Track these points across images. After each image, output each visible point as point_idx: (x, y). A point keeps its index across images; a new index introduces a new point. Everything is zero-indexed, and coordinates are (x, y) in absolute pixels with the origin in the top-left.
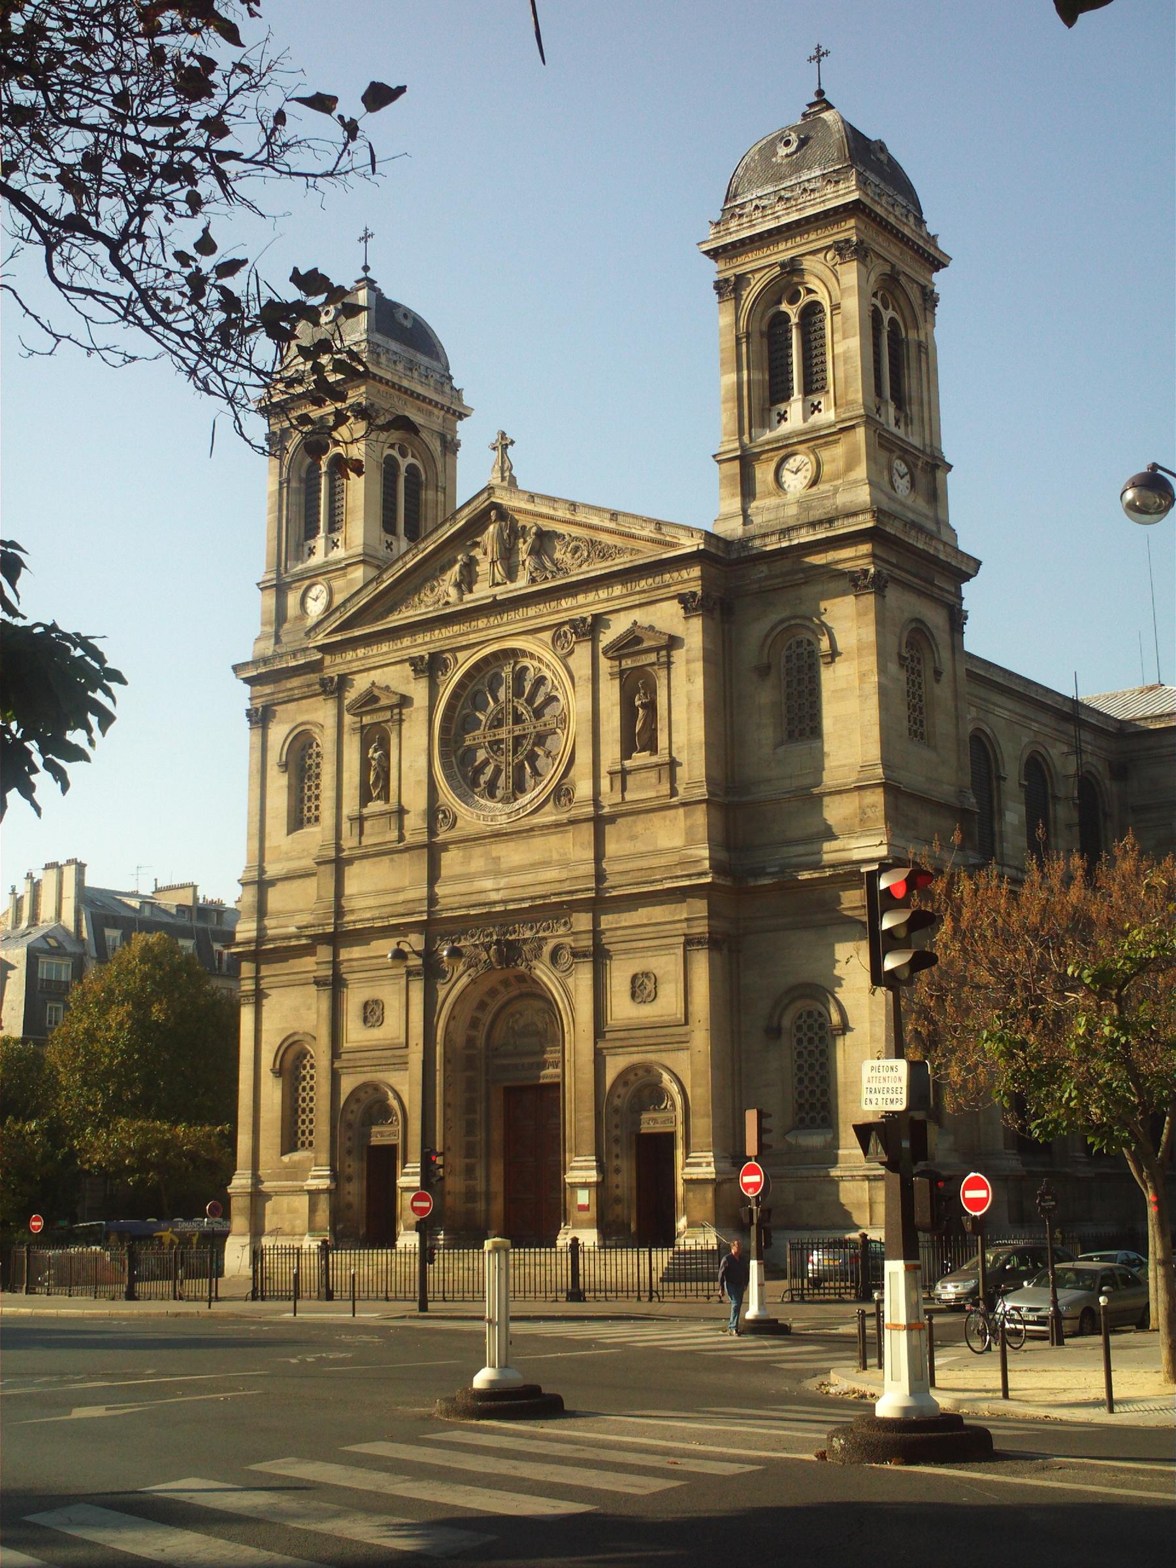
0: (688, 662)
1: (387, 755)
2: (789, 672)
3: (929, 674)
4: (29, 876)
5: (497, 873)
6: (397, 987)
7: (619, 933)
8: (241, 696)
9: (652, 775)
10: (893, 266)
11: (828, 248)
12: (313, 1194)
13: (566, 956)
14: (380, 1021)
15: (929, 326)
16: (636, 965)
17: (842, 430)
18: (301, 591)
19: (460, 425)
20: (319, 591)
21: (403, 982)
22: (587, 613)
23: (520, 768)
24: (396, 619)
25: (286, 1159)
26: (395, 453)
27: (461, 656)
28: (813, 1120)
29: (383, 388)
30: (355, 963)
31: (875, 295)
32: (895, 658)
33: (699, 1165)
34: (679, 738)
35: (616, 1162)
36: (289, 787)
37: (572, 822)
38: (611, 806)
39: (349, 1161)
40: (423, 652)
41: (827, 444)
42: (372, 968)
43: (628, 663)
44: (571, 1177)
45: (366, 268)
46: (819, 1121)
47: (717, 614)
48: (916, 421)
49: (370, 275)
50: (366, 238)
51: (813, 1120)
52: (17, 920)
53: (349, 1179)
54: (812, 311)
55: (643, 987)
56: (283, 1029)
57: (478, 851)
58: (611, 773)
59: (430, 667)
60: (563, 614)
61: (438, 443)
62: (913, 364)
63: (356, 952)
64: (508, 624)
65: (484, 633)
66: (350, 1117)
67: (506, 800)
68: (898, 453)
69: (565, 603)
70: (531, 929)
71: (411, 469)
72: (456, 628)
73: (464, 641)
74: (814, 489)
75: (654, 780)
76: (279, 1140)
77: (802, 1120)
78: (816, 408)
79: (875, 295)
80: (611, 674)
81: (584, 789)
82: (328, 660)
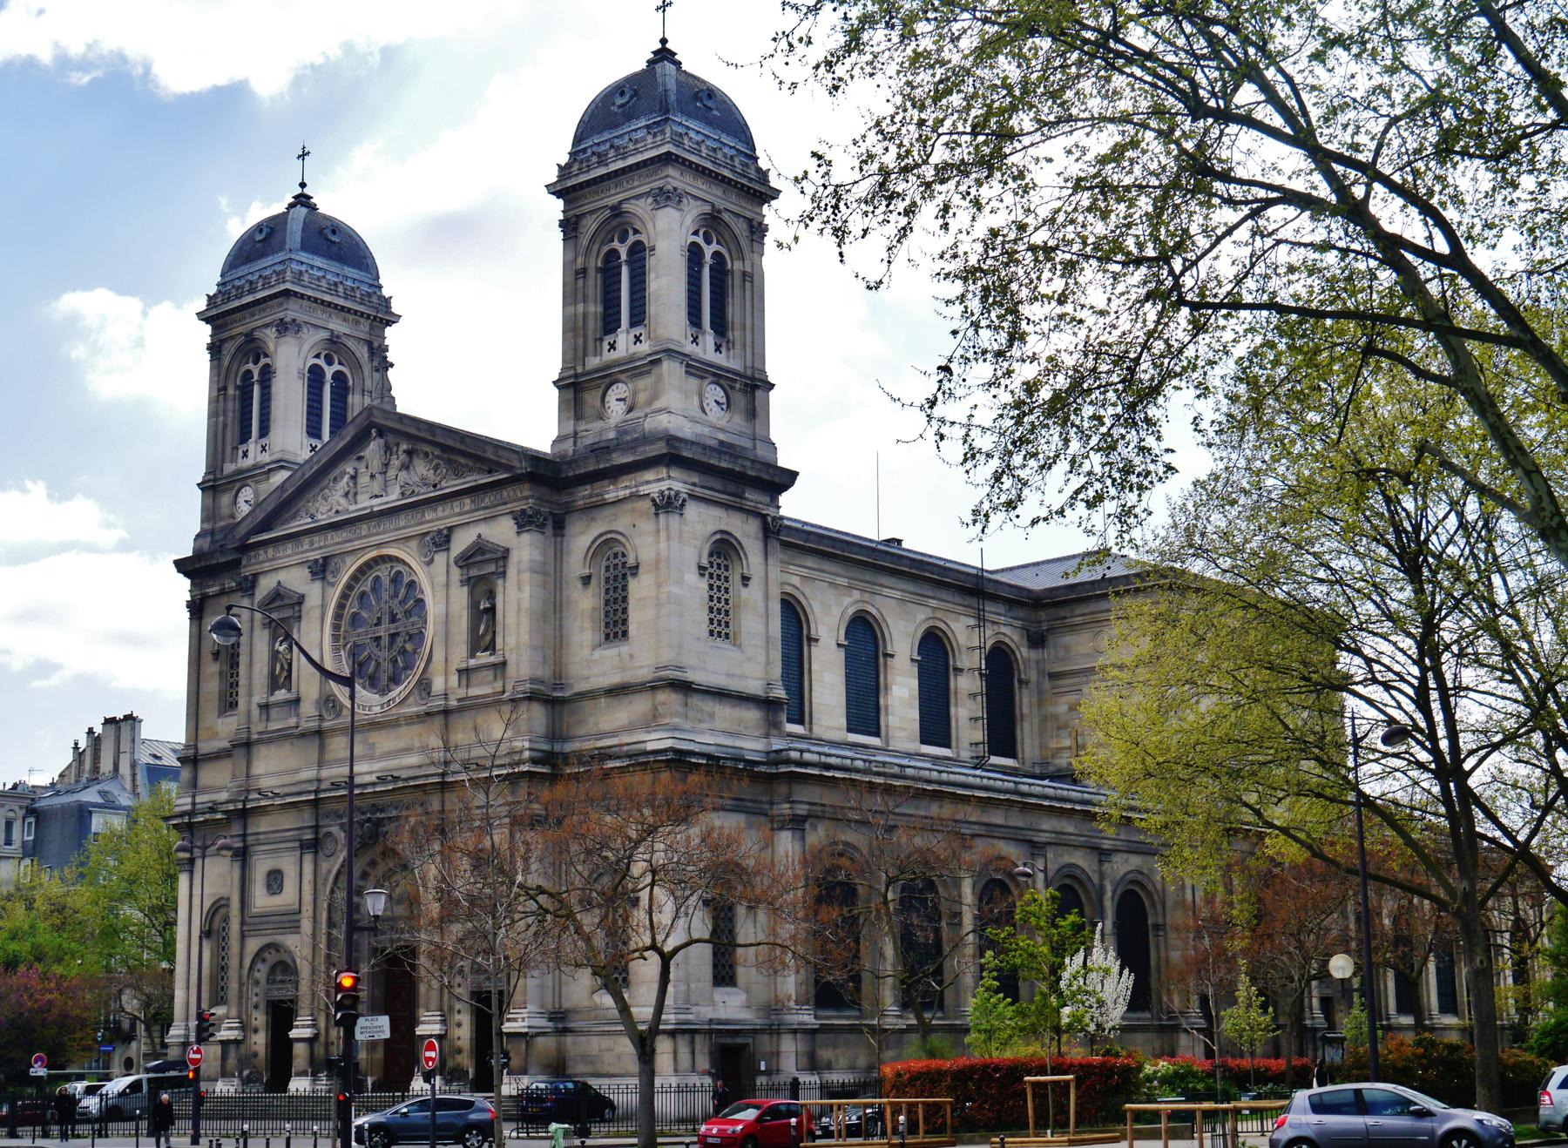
0: (519, 572)
2: (607, 579)
3: (735, 579)
4: (91, 731)
8: (182, 587)
9: (489, 674)
10: (713, 206)
11: (647, 194)
12: (225, 1044)
14: (281, 888)
15: (756, 256)
17: (652, 362)
19: (389, 331)
20: (247, 493)
21: (298, 853)
22: (442, 524)
24: (301, 523)
26: (321, 362)
27: (349, 560)
29: (305, 303)
31: (696, 233)
32: (695, 569)
33: (515, 1020)
34: (511, 640)
35: (457, 1017)
36: (221, 673)
38: (459, 700)
39: (255, 1014)
40: (315, 555)
41: (641, 374)
42: (276, 841)
43: (474, 572)
44: (421, 1030)
45: (303, 185)
47: (549, 530)
48: (738, 346)
49: (306, 191)
50: (303, 155)
52: (79, 775)
53: (256, 1031)
54: (639, 252)
59: (321, 570)
61: (365, 349)
62: (737, 292)
63: (261, 825)
64: (384, 533)
66: (257, 975)
67: (383, 692)
68: (711, 379)
69: (429, 516)
71: (338, 376)
73: (349, 547)
74: (631, 415)
78: (638, 339)
79: (696, 233)
81: (438, 685)
82: (244, 562)
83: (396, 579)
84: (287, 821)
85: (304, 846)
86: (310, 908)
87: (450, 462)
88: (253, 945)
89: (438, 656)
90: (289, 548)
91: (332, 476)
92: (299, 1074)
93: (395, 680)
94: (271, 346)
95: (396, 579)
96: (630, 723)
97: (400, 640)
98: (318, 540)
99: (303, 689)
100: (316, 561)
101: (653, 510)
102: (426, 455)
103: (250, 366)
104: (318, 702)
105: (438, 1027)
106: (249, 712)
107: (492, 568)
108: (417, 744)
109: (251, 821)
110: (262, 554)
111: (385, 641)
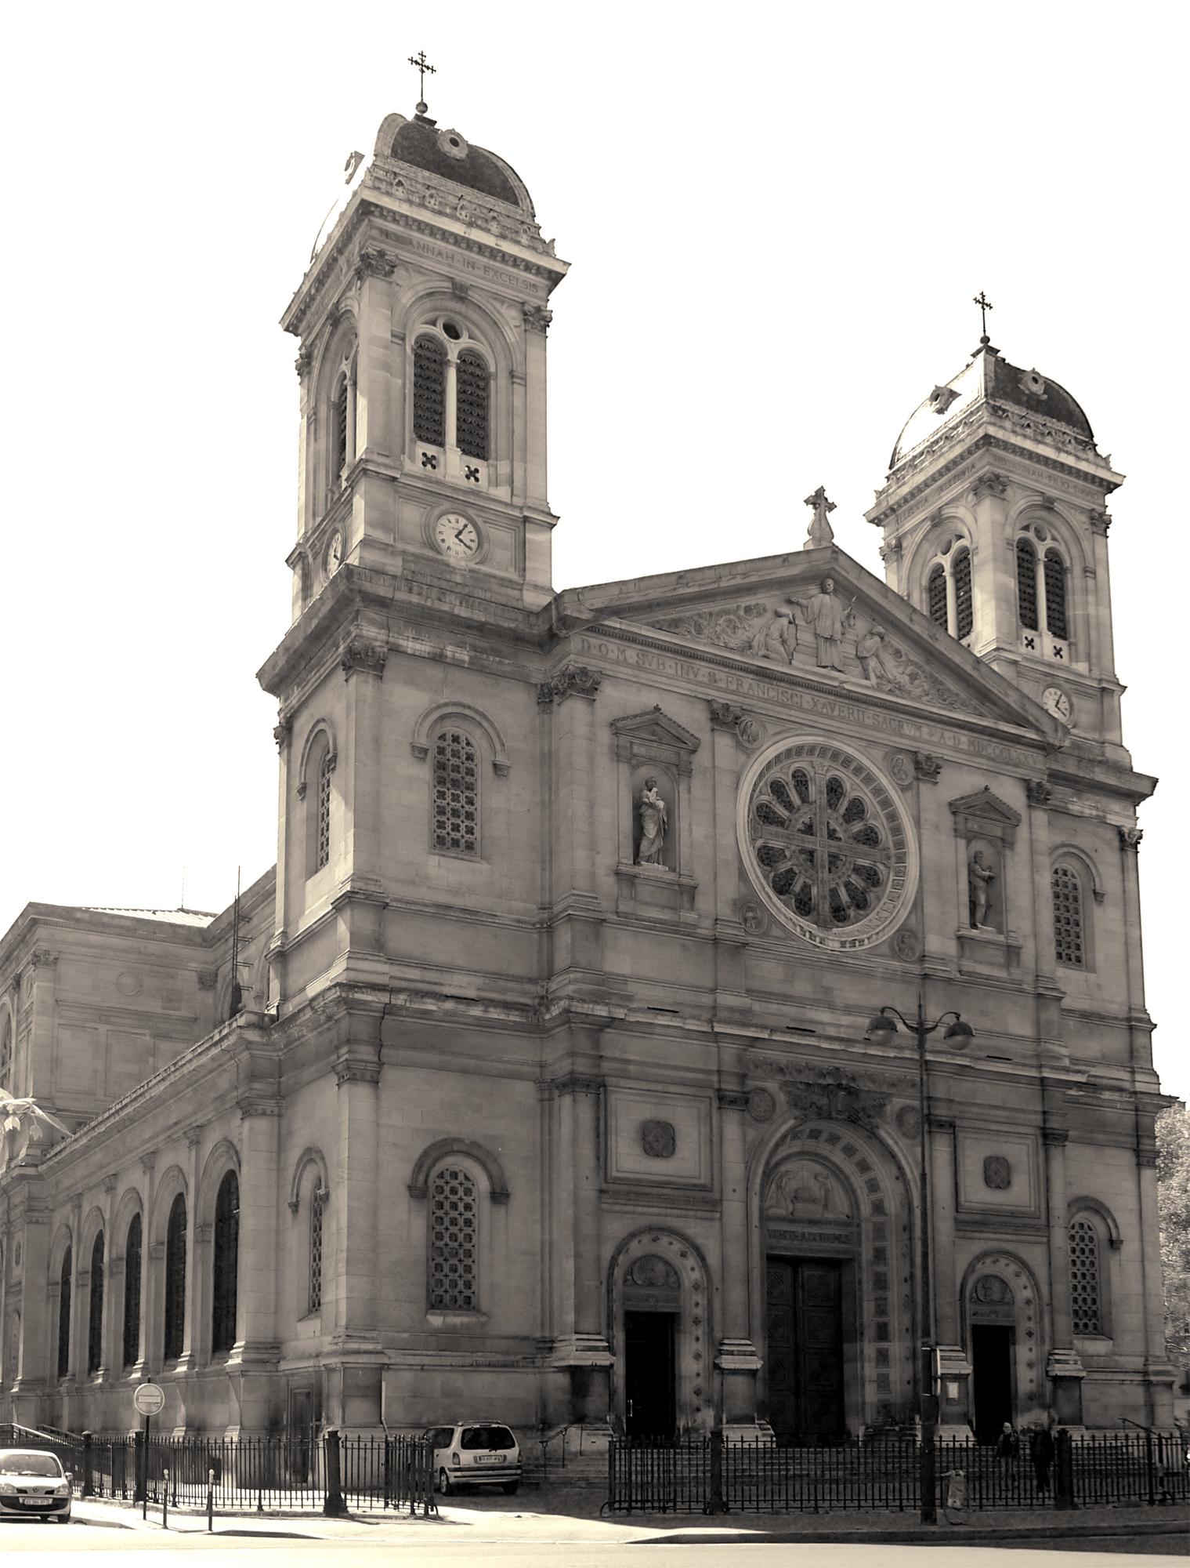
0: (1032, 852)
1: (670, 811)
5: (831, 1007)
7: (975, 1110)
16: (990, 1148)
21: (704, 1107)
28: (1086, 1326)
30: (632, 1068)
43: (973, 825)
46: (1091, 1328)
51: (1086, 1326)
55: (997, 1173)
58: (959, 938)
60: (906, 741)
65: (811, 717)
70: (874, 1082)
72: (772, 693)
75: (1002, 960)
77: (1076, 1325)
80: (955, 830)
85: (724, 1100)
88: (616, 1228)
89: (931, 907)
90: (671, 665)
92: (736, 1420)
93: (839, 915)
96: (1103, 1056)
99: (702, 876)
100: (727, 707)
104: (735, 903)
106: (592, 876)
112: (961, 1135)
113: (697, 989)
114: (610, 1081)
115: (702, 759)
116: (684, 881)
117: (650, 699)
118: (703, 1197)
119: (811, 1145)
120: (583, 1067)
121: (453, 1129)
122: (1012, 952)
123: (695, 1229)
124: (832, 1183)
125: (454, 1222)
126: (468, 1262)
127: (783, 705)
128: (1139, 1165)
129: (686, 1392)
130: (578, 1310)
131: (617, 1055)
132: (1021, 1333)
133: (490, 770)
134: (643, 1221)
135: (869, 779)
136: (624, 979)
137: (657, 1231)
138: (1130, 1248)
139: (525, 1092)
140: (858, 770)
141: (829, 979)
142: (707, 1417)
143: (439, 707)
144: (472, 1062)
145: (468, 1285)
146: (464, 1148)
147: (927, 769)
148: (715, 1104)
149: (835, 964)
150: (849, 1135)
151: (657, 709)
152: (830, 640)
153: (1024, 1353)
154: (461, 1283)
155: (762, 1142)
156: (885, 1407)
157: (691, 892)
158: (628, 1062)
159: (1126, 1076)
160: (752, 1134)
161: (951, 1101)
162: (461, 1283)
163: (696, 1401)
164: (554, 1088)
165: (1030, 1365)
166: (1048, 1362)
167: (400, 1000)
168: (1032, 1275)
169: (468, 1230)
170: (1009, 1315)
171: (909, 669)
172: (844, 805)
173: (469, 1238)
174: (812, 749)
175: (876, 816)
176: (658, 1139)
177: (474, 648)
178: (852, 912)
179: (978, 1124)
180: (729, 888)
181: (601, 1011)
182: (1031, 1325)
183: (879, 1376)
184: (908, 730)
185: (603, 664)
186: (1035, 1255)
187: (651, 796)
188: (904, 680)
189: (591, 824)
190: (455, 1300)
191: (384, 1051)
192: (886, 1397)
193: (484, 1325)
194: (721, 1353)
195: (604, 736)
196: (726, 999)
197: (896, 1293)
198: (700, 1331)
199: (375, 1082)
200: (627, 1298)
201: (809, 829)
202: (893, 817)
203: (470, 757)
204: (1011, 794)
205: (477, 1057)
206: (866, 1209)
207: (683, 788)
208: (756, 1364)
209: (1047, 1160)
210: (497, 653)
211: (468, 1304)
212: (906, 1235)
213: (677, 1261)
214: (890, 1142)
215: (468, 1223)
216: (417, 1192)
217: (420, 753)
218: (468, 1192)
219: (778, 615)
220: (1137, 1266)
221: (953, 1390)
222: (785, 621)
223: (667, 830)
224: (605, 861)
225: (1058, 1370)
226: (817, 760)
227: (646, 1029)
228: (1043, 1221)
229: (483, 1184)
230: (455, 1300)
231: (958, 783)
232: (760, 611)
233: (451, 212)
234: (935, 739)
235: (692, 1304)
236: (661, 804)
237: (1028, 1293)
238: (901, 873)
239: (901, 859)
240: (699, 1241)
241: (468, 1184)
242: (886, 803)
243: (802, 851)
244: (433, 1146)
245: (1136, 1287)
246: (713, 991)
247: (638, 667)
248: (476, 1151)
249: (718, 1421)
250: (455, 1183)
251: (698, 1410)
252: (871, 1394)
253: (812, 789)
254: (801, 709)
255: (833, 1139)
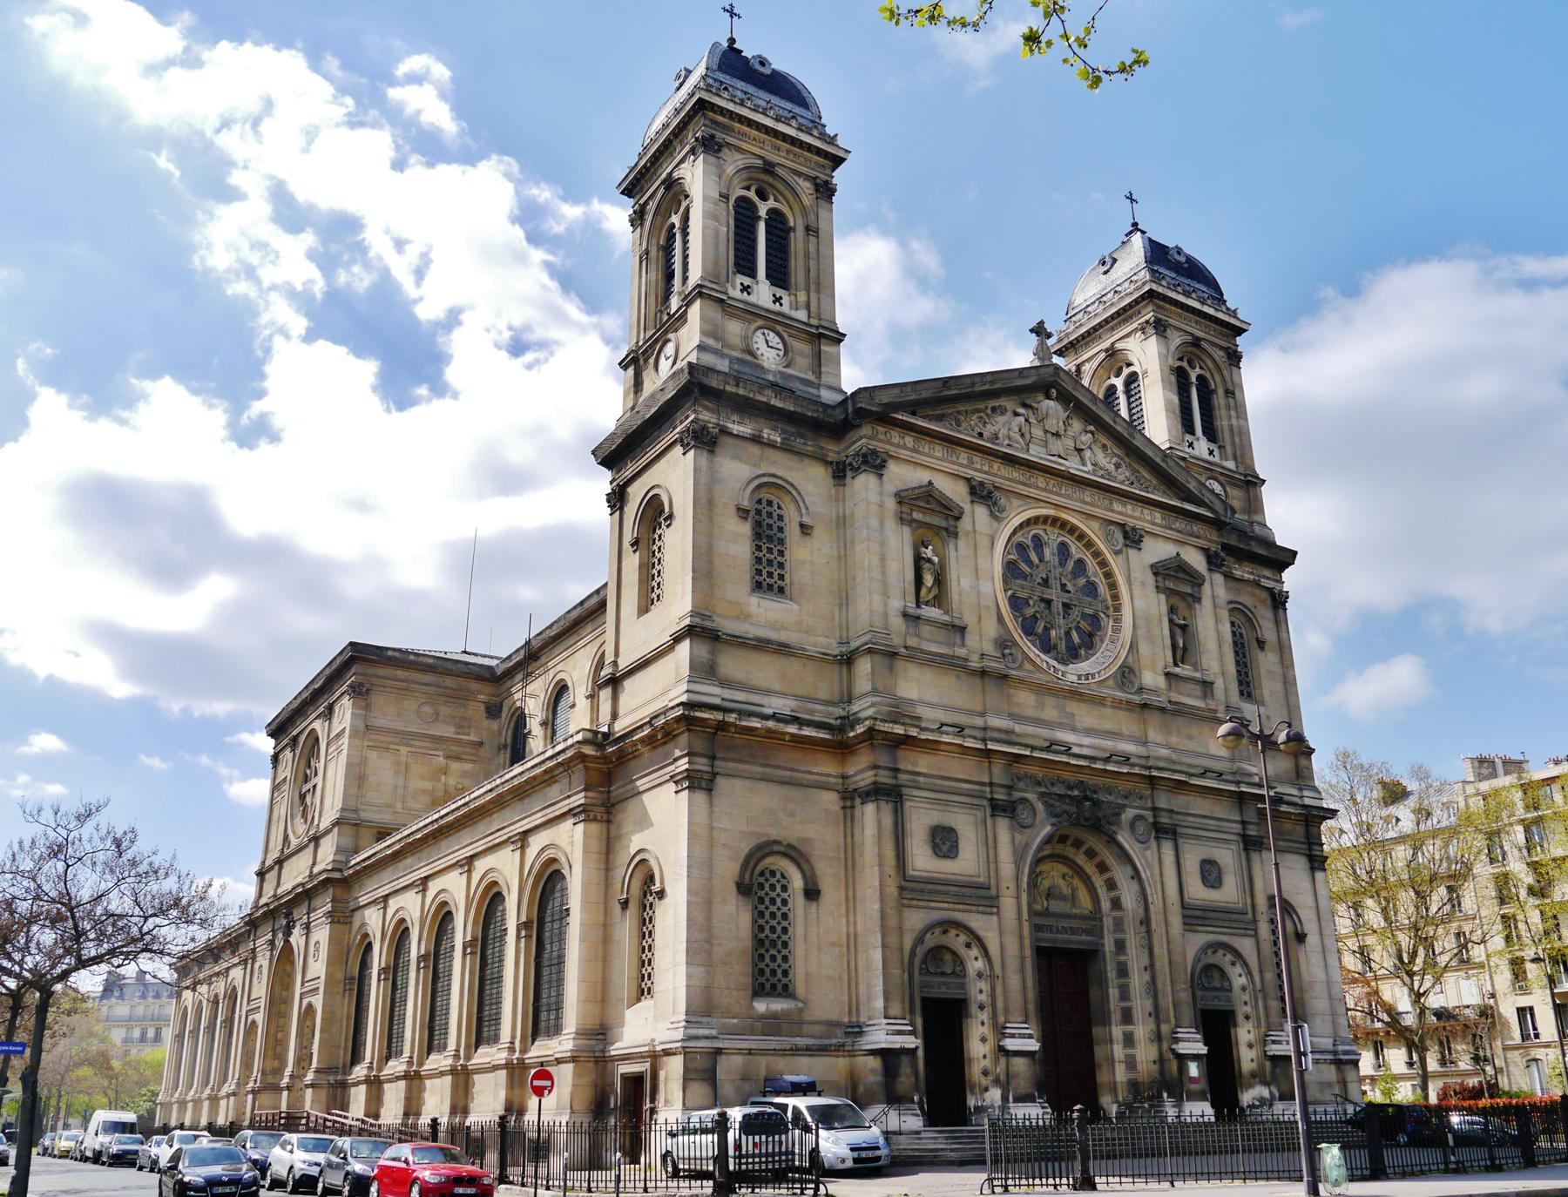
0: (1215, 606)
5: (1074, 729)
6: (972, 819)
12: (888, 1057)
13: (1141, 827)
18: (753, 327)
22: (1139, 524)
23: (1068, 633)
25: (761, 1006)
27: (1016, 502)
30: (921, 779)
33: (1279, 1042)
37: (1145, 706)
42: (943, 791)
55: (1211, 873)
56: (752, 834)
57: (1050, 701)
63: (923, 763)
64: (1068, 497)
75: (1199, 693)
76: (750, 980)
83: (1063, 550)
84: (966, 770)
85: (997, 808)
86: (1012, 885)
87: (1134, 471)
88: (916, 919)
89: (1144, 648)
90: (939, 451)
91: (991, 403)
94: (807, 200)
95: (1063, 550)
97: (1075, 613)
98: (978, 460)
99: (969, 619)
100: (982, 484)
101: (1269, 602)
102: (1104, 447)
103: (752, 194)
105: (1201, 1045)
107: (1188, 589)
108: (1126, 732)
109: (901, 753)
110: (895, 436)
111: (1057, 606)
112: (1180, 841)
113: (971, 713)
114: (905, 791)
115: (965, 524)
116: (957, 622)
117: (922, 476)
118: (982, 895)
119: (1059, 848)
120: (885, 778)
121: (774, 834)
122: (1207, 686)
123: (976, 922)
124: (1076, 881)
125: (773, 915)
126: (785, 952)
127: (1024, 484)
128: (1313, 869)
129: (975, 1072)
130: (887, 997)
131: (910, 768)
132: (1240, 1018)
133: (798, 528)
134: (936, 916)
135: (1089, 544)
136: (912, 702)
137: (947, 925)
138: (1312, 940)
139: (830, 800)
140: (1081, 537)
141: (1071, 706)
142: (995, 1095)
143: (758, 477)
144: (788, 773)
145: (785, 973)
146: (782, 849)
147: (1133, 538)
148: (988, 812)
149: (1075, 694)
150: (1092, 841)
151: (930, 483)
152: (1057, 435)
153: (1244, 1034)
154: (779, 972)
155: (1027, 846)
156: (1134, 1086)
157: (962, 630)
158: (918, 774)
159: (1295, 792)
160: (1018, 837)
161: (1172, 811)
162: (779, 972)
163: (985, 1081)
164: (851, 797)
165: (1250, 1046)
166: (1265, 1043)
167: (731, 718)
168: (1245, 964)
169: (785, 924)
170: (1229, 1000)
171: (1115, 460)
172: (1070, 565)
173: (785, 930)
174: (1045, 519)
175: (1096, 574)
176: (944, 841)
177: (783, 432)
178: (1083, 652)
179: (1192, 831)
180: (991, 629)
181: (899, 730)
182: (1248, 1009)
183: (1127, 1056)
184: (1117, 506)
185: (888, 447)
186: (1246, 946)
187: (928, 552)
188: (1111, 468)
189: (883, 573)
190: (774, 986)
191: (717, 763)
192: (1132, 1076)
193: (801, 1010)
194: (1004, 1036)
195: (891, 504)
196: (995, 722)
197: (1137, 980)
198: (984, 1016)
199: (709, 790)
200: (924, 985)
201: (1045, 582)
202: (1109, 575)
203: (781, 518)
204: (1196, 560)
205: (792, 770)
206: (1106, 905)
207: (951, 546)
208: (1033, 1045)
209: (1249, 860)
210: (802, 436)
211: (786, 992)
212: (1143, 928)
213: (962, 951)
214: (1127, 846)
215: (785, 916)
216: (744, 889)
217: (743, 513)
218: (784, 888)
219: (1016, 414)
220: (1320, 956)
221: (1193, 1070)
222: (1022, 419)
223: (940, 580)
224: (896, 604)
225: (1274, 1050)
226: (1049, 529)
227: (932, 746)
228: (1250, 915)
229: (797, 882)
230: (774, 986)
231: (1158, 550)
232: (1003, 411)
233: (735, 98)
234: (1137, 514)
235: (978, 991)
236: (936, 559)
237: (1243, 980)
238: (1118, 620)
239: (1117, 609)
240: (981, 933)
241: (784, 882)
242: (1103, 564)
243: (1042, 600)
244: (759, 847)
245: (1321, 975)
246: (983, 714)
247: (914, 450)
248: (794, 853)
249: (1005, 1099)
250: (773, 881)
251: (986, 1090)
252: (1121, 1075)
253: (1047, 552)
254: (1037, 488)
255: (1078, 844)
